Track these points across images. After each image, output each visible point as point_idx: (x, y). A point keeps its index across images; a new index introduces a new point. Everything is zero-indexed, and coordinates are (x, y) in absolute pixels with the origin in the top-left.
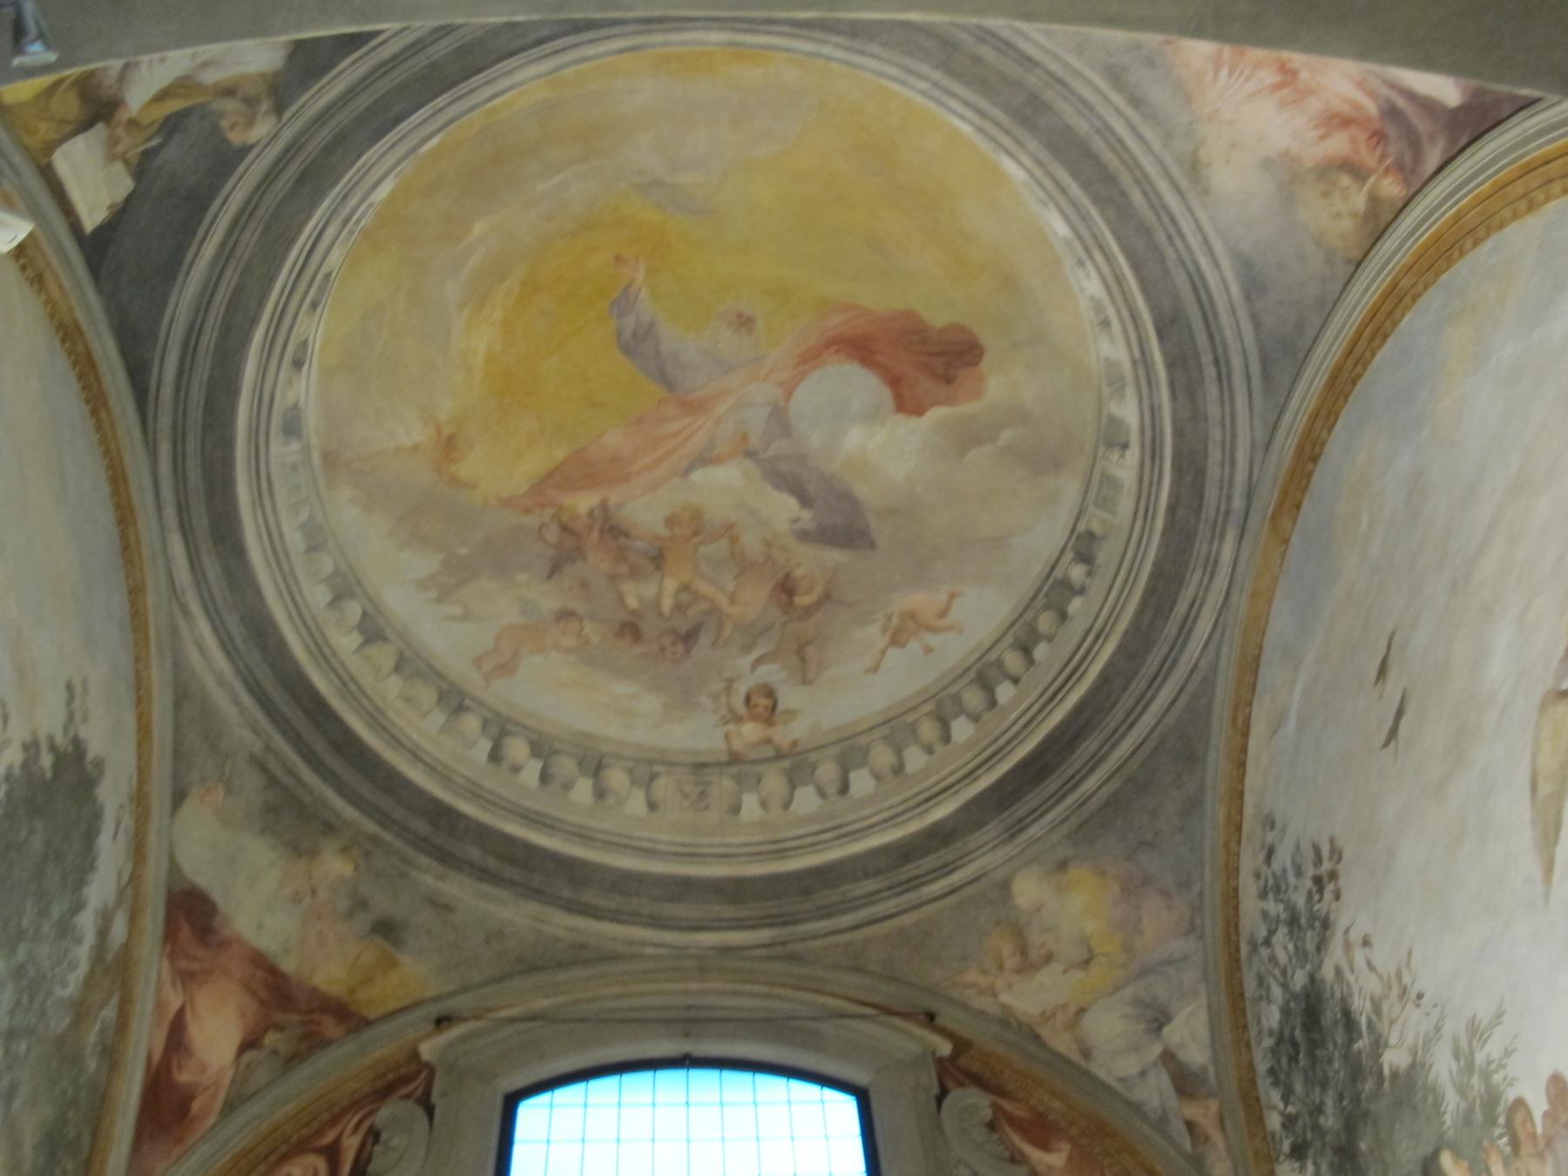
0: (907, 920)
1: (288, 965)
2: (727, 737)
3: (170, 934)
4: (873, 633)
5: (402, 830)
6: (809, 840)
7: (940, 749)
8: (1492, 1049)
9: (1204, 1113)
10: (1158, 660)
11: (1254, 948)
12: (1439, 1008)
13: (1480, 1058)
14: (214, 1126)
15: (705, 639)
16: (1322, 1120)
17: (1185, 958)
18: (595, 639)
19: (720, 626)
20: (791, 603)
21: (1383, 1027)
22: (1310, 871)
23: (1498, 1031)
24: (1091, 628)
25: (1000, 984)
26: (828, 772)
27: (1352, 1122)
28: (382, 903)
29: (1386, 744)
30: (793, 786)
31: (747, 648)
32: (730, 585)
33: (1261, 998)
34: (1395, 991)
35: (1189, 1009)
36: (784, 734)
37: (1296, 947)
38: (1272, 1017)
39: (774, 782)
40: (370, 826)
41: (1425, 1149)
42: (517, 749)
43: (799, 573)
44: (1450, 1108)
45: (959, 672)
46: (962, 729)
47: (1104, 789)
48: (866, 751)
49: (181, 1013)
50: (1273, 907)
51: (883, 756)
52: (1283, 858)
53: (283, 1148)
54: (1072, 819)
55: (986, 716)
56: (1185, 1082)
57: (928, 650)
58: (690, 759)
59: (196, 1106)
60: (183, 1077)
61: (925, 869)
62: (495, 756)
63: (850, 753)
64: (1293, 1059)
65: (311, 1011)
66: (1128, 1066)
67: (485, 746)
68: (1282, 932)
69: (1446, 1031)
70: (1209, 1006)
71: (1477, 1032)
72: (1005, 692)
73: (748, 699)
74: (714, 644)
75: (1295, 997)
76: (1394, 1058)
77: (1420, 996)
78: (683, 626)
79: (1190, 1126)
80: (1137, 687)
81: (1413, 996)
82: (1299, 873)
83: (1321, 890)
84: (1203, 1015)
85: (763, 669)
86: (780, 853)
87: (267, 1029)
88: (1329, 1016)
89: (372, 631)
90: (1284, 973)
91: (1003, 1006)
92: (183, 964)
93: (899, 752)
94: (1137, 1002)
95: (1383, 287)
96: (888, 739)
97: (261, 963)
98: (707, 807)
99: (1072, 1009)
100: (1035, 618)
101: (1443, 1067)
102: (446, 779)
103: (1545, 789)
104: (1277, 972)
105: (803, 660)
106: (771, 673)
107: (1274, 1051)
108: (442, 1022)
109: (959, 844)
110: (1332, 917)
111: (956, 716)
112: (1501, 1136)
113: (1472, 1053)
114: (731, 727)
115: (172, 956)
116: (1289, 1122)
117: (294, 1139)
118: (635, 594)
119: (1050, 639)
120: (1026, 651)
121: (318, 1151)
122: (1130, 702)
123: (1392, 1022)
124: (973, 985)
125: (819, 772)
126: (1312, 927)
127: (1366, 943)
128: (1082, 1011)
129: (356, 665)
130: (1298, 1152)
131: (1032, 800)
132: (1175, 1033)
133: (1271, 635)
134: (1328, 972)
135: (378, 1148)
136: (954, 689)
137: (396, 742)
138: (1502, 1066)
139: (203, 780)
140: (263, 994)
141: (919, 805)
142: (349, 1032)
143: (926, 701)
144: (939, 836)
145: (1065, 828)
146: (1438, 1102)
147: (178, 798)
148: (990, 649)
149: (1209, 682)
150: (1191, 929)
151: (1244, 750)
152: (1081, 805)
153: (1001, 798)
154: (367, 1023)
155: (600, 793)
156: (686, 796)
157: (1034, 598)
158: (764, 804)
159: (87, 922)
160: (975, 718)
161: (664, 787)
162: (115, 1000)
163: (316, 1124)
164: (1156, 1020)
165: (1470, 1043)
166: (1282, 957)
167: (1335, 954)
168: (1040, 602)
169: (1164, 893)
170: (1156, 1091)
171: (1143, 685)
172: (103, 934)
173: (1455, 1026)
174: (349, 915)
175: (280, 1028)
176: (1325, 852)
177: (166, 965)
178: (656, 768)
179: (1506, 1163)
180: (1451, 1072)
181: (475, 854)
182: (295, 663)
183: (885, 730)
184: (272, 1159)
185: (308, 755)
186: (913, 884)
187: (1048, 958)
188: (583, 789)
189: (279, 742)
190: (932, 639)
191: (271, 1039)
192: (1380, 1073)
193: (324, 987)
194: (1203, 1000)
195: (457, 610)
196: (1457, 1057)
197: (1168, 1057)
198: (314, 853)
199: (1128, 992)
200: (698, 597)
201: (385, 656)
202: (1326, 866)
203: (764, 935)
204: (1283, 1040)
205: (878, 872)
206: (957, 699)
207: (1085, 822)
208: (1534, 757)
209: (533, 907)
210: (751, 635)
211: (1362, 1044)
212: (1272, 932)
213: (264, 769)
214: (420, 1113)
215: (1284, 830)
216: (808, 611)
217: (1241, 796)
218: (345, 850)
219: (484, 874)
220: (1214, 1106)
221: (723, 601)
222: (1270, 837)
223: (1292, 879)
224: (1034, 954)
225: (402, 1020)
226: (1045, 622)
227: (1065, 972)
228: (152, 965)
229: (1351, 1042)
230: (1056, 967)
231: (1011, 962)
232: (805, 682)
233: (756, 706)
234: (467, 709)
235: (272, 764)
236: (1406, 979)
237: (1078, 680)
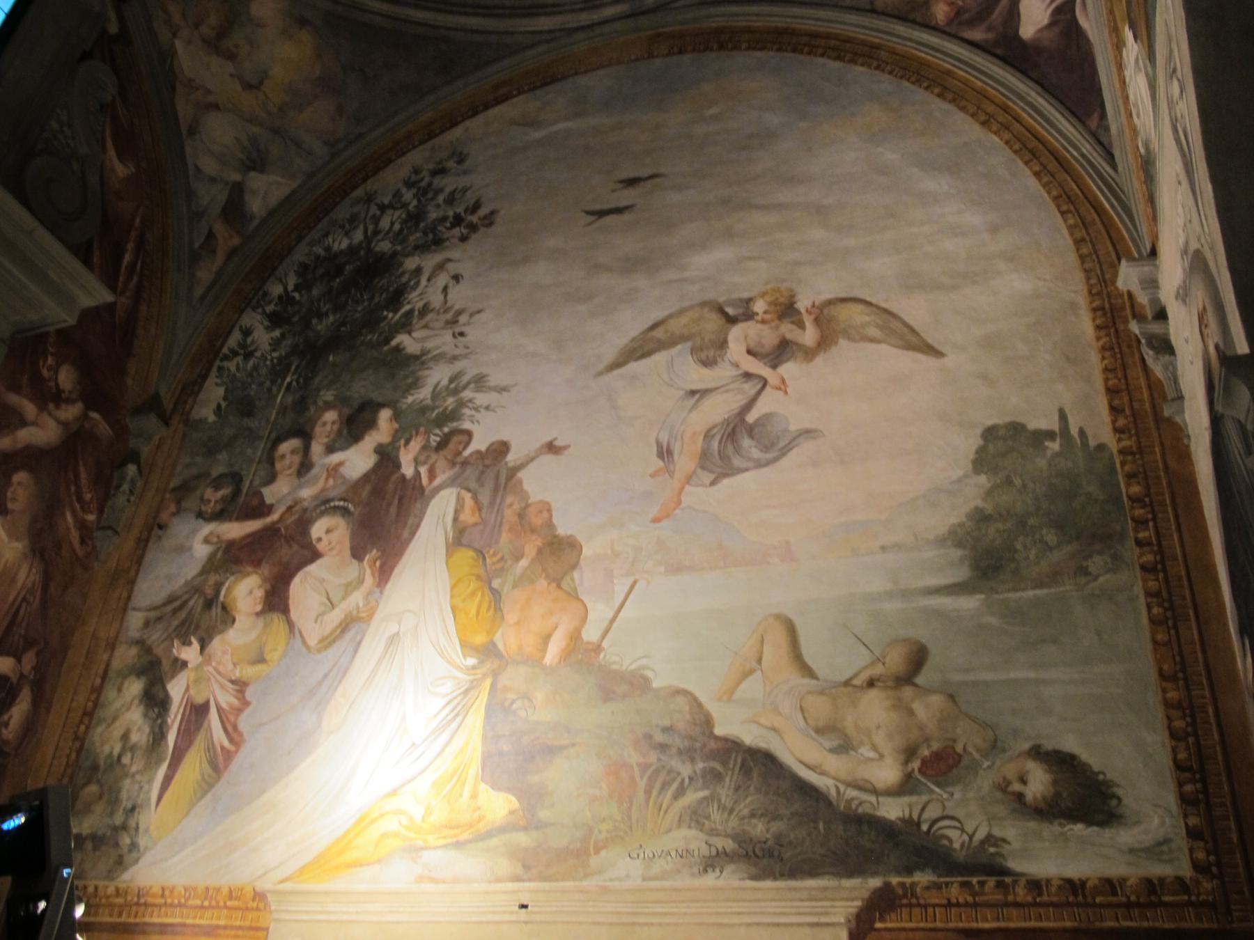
8: (481, 399)
9: (227, 239)
11: (369, 199)
12: (468, 351)
13: (467, 394)
16: (315, 321)
22: (460, 210)
23: (494, 395)
27: (334, 341)
29: (589, 213)
33: (342, 227)
34: (449, 316)
35: (278, 179)
37: (401, 230)
38: (341, 243)
41: (376, 396)
44: (416, 396)
50: (408, 195)
52: (449, 183)
66: (210, 166)
69: (459, 365)
70: (294, 192)
71: (479, 382)
75: (369, 251)
76: (408, 343)
77: (462, 334)
79: (211, 235)
81: (457, 330)
82: (450, 200)
83: (453, 226)
84: (286, 191)
90: (376, 233)
91: (173, 46)
95: (871, 39)
99: (211, 99)
101: (437, 376)
103: (659, 333)
104: (371, 228)
110: (447, 243)
112: (436, 435)
113: (464, 388)
116: (285, 299)
123: (426, 327)
126: (425, 234)
127: (457, 278)
128: (216, 107)
132: (256, 181)
133: (583, 81)
134: (411, 263)
138: (476, 409)
151: (487, 107)
165: (469, 383)
166: (385, 223)
167: (429, 261)
170: (211, 197)
173: (470, 369)
176: (483, 212)
179: (425, 448)
180: (438, 384)
187: (231, 57)
192: (387, 341)
194: (294, 185)
196: (451, 381)
197: (238, 190)
199: (256, 130)
202: (474, 219)
208: (670, 316)
211: (393, 317)
212: (391, 206)
215: (466, 172)
217: (454, 124)
220: (236, 241)
222: (451, 164)
223: (441, 198)
227: (231, 75)
229: (387, 308)
230: (229, 67)
236: (463, 319)
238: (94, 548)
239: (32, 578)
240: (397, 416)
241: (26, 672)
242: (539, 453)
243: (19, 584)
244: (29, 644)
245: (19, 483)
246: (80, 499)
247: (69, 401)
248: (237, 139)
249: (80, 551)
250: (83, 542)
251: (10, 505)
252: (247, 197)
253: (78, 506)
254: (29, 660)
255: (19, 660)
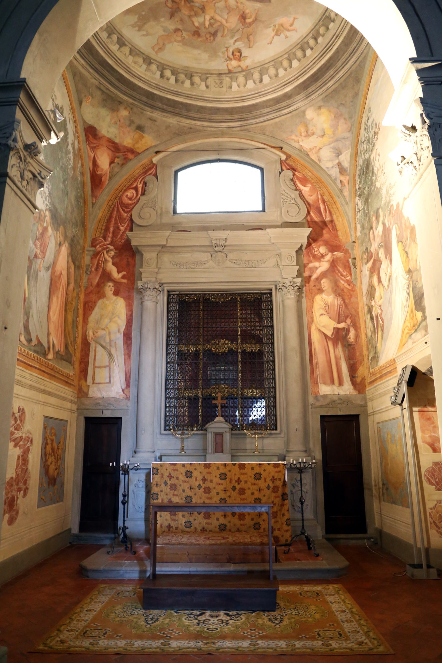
0: (277, 120)
1: (117, 141)
2: (227, 65)
3: (87, 139)
4: (270, 32)
5: (140, 100)
6: (251, 96)
7: (288, 69)
9: (345, 179)
10: (353, 47)
11: (361, 143)
13: (390, 192)
14: (108, 183)
15: (219, 34)
17: (348, 138)
18: (187, 37)
19: (224, 30)
20: (245, 21)
21: (378, 176)
24: (335, 33)
25: (300, 140)
26: (256, 76)
27: (369, 194)
28: (138, 122)
30: (246, 80)
31: (232, 37)
32: (226, 17)
34: (381, 170)
36: (244, 64)
38: (361, 163)
39: (241, 79)
40: (131, 101)
42: (168, 73)
43: (247, 11)
45: (296, 44)
46: (295, 63)
47: (333, 86)
48: (267, 69)
49: (94, 156)
51: (272, 71)
53: (125, 188)
54: (324, 94)
55: (302, 59)
56: (342, 170)
57: (287, 37)
58: (217, 72)
59: (103, 179)
60: (99, 173)
61: (282, 106)
62: (162, 76)
63: (263, 71)
64: (363, 174)
65: (125, 152)
66: (329, 165)
67: (159, 73)
68: (366, 142)
72: (308, 52)
73: (233, 53)
74: (222, 36)
76: (378, 184)
77: (384, 173)
78: (212, 30)
79: (341, 181)
80: (346, 55)
82: (372, 129)
84: (349, 154)
85: (237, 44)
86: (243, 100)
87: (115, 158)
88: (370, 168)
89: (121, 43)
91: (301, 146)
92: (92, 145)
93: (277, 70)
94: (334, 148)
96: (274, 66)
97: (110, 141)
98: (222, 87)
99: (318, 148)
100: (319, 28)
101: (384, 192)
102: (149, 85)
105: (249, 40)
106: (239, 45)
107: (360, 170)
108: (157, 152)
109: (292, 99)
111: (294, 59)
114: (228, 62)
115: (89, 144)
116: (360, 188)
117: (127, 186)
118: (197, 21)
119: (323, 36)
120: (316, 39)
121: (133, 188)
122: (344, 60)
124: (293, 140)
125: (254, 76)
127: (379, 155)
128: (320, 148)
129: (119, 54)
130: (360, 196)
131: (313, 88)
135: (146, 188)
136: (294, 50)
137: (134, 76)
139: (85, 96)
140: (113, 149)
141: (282, 87)
142: (135, 156)
143: (285, 54)
144: (287, 96)
145: (321, 97)
146: (382, 198)
147: (81, 103)
148: (305, 37)
149: (365, 58)
150: (350, 130)
151: (369, 84)
152: (326, 90)
153: (305, 86)
154: (139, 154)
155: (192, 84)
156: (216, 84)
157: (320, 21)
158: (239, 86)
159: (70, 148)
160: (299, 60)
161: (210, 81)
162: (80, 161)
163: (131, 182)
164: (338, 153)
168: (321, 23)
169: (345, 119)
170: (335, 172)
171: (348, 55)
172: (74, 148)
174: (130, 125)
175: (118, 157)
177: (88, 147)
178: (207, 76)
181: (160, 105)
182: (102, 57)
183: (273, 63)
184: (123, 191)
185: (111, 83)
186: (280, 109)
187: (313, 134)
188: (187, 83)
189: (102, 81)
190: (288, 34)
191: (116, 160)
193: (126, 145)
194: (350, 150)
195: (145, 33)
197: (339, 164)
198: (118, 110)
199: (332, 145)
200: (216, 21)
201: (126, 50)
203: (239, 123)
204: (362, 169)
205: (270, 106)
206: (294, 54)
207: (327, 95)
209: (178, 118)
210: (233, 32)
211: (374, 178)
212: (365, 141)
213: (100, 89)
214: (155, 179)
216: (250, 24)
218: (125, 108)
219: (163, 110)
220: (348, 178)
221: (224, 22)
224: (310, 132)
225: (147, 152)
226: (322, 30)
228: (86, 148)
230: (315, 136)
231: (303, 134)
232: (249, 48)
233: (235, 55)
234: (152, 63)
235: (102, 87)
236: (383, 168)
237: (330, 50)
238: (354, 285)
239: (339, 302)
240: (382, 210)
241: (349, 324)
242: (404, 202)
243: (336, 305)
244: (346, 317)
245: (324, 283)
246: (342, 276)
247: (327, 254)
248: (330, 152)
249: (350, 288)
250: (349, 285)
251: (324, 289)
252: (342, 164)
253: (343, 278)
254: (349, 321)
255: (346, 322)
